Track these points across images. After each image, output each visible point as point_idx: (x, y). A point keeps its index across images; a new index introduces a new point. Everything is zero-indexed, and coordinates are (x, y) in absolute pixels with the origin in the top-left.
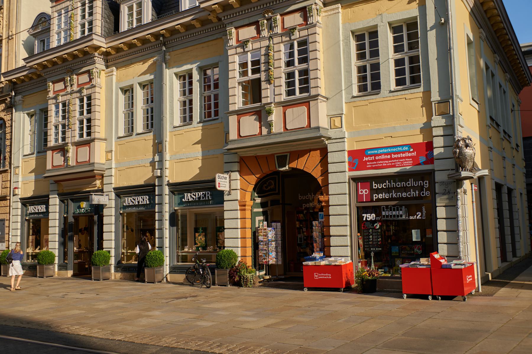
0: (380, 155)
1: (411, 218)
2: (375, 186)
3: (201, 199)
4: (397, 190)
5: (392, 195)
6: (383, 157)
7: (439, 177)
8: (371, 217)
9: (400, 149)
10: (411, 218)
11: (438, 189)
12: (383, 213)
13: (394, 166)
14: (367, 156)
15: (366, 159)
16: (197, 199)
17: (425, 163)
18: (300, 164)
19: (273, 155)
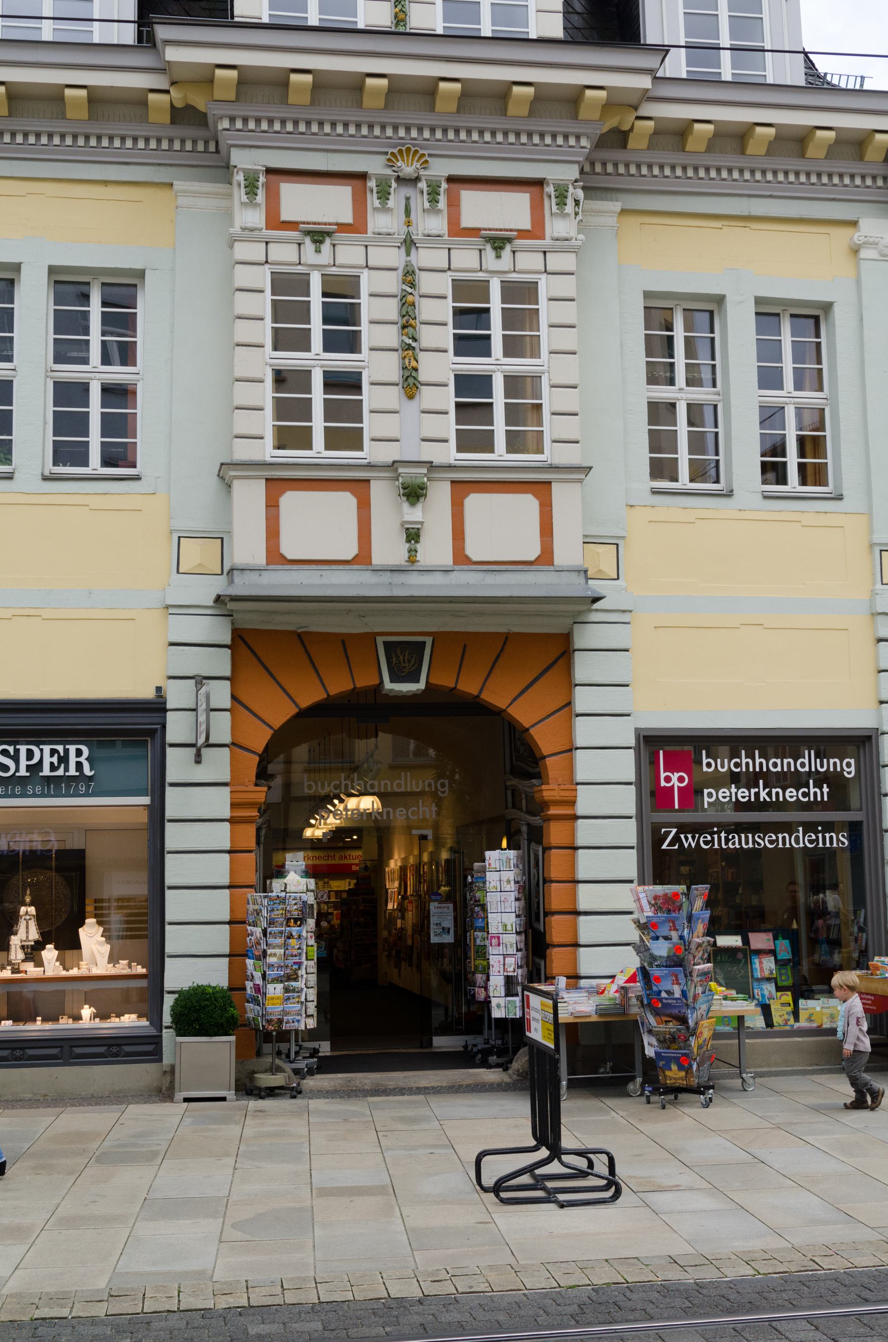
3: (46, 771)
5: (757, 795)
16: (23, 772)
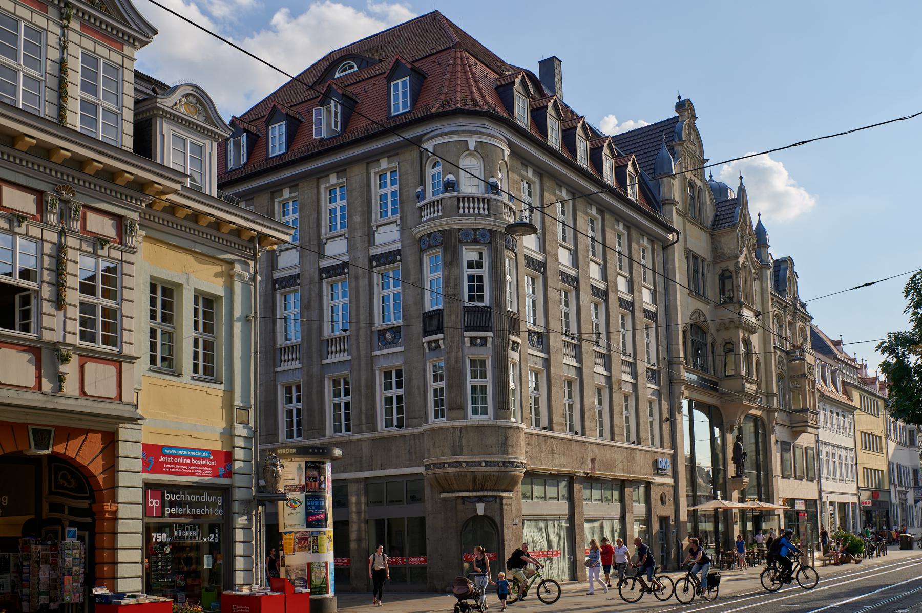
0: (179, 457)
1: (204, 540)
2: (168, 497)
4: (191, 505)
6: (182, 460)
7: (238, 494)
8: (161, 537)
9: (200, 454)
10: (204, 540)
11: (236, 507)
12: (176, 533)
13: (193, 474)
14: (164, 456)
15: (162, 459)
17: (224, 476)
18: (71, 449)
19: (25, 425)
